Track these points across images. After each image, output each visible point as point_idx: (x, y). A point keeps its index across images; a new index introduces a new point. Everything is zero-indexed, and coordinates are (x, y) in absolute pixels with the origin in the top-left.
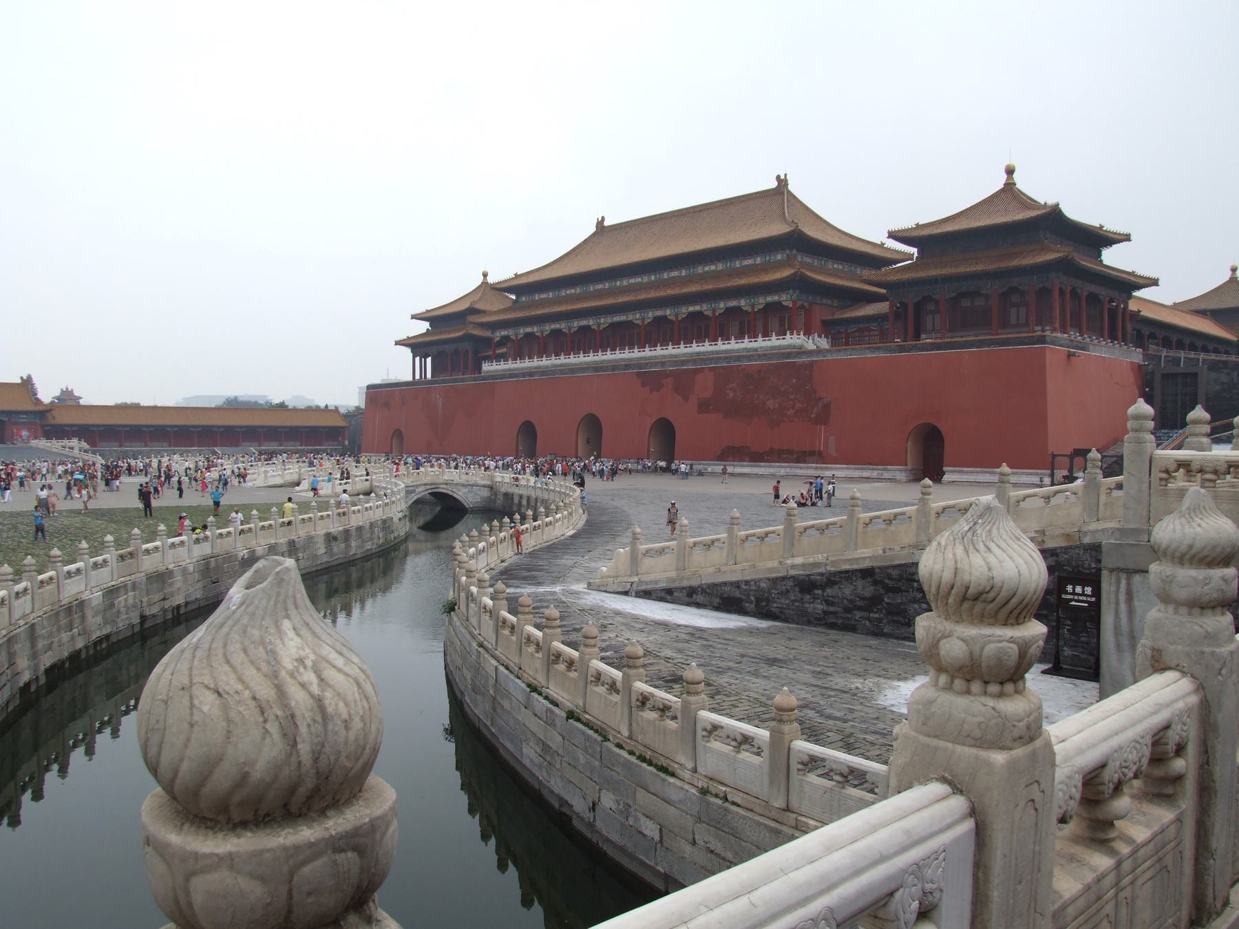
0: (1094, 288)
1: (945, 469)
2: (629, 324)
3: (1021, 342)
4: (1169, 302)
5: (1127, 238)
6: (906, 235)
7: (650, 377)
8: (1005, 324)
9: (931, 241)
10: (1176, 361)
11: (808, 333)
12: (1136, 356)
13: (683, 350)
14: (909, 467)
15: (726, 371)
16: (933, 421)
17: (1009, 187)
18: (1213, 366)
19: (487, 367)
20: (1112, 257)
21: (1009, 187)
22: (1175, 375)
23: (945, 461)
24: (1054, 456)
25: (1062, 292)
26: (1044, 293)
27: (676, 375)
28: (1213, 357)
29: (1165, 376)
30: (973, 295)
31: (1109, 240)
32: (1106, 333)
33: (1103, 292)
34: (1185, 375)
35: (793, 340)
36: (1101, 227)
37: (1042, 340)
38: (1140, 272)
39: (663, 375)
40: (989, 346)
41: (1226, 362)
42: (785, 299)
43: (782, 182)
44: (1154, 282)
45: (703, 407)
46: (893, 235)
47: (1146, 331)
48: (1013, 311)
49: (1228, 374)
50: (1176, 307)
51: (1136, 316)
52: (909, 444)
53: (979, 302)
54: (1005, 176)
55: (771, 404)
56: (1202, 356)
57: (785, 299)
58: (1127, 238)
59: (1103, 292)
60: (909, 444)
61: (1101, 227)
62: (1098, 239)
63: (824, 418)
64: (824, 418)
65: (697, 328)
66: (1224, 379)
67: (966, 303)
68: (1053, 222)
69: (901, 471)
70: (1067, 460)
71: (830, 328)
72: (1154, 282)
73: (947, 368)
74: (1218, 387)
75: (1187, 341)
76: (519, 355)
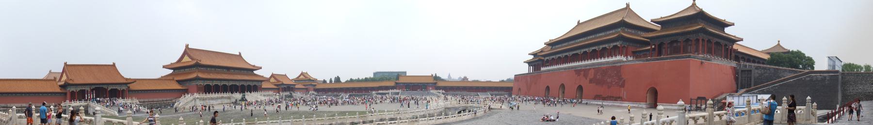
2: (577, 54)
3: (683, 57)
7: (578, 71)
8: (685, 51)
9: (665, 23)
11: (626, 55)
13: (583, 63)
15: (598, 69)
19: (543, 69)
25: (703, 40)
26: (698, 40)
27: (584, 70)
30: (676, 41)
35: (618, 58)
39: (581, 71)
42: (618, 44)
43: (628, 5)
45: (591, 81)
55: (609, 80)
57: (618, 44)
63: (623, 86)
64: (623, 86)
65: (595, 55)
67: (675, 45)
68: (701, 16)
71: (635, 54)
73: (663, 67)
76: (551, 65)
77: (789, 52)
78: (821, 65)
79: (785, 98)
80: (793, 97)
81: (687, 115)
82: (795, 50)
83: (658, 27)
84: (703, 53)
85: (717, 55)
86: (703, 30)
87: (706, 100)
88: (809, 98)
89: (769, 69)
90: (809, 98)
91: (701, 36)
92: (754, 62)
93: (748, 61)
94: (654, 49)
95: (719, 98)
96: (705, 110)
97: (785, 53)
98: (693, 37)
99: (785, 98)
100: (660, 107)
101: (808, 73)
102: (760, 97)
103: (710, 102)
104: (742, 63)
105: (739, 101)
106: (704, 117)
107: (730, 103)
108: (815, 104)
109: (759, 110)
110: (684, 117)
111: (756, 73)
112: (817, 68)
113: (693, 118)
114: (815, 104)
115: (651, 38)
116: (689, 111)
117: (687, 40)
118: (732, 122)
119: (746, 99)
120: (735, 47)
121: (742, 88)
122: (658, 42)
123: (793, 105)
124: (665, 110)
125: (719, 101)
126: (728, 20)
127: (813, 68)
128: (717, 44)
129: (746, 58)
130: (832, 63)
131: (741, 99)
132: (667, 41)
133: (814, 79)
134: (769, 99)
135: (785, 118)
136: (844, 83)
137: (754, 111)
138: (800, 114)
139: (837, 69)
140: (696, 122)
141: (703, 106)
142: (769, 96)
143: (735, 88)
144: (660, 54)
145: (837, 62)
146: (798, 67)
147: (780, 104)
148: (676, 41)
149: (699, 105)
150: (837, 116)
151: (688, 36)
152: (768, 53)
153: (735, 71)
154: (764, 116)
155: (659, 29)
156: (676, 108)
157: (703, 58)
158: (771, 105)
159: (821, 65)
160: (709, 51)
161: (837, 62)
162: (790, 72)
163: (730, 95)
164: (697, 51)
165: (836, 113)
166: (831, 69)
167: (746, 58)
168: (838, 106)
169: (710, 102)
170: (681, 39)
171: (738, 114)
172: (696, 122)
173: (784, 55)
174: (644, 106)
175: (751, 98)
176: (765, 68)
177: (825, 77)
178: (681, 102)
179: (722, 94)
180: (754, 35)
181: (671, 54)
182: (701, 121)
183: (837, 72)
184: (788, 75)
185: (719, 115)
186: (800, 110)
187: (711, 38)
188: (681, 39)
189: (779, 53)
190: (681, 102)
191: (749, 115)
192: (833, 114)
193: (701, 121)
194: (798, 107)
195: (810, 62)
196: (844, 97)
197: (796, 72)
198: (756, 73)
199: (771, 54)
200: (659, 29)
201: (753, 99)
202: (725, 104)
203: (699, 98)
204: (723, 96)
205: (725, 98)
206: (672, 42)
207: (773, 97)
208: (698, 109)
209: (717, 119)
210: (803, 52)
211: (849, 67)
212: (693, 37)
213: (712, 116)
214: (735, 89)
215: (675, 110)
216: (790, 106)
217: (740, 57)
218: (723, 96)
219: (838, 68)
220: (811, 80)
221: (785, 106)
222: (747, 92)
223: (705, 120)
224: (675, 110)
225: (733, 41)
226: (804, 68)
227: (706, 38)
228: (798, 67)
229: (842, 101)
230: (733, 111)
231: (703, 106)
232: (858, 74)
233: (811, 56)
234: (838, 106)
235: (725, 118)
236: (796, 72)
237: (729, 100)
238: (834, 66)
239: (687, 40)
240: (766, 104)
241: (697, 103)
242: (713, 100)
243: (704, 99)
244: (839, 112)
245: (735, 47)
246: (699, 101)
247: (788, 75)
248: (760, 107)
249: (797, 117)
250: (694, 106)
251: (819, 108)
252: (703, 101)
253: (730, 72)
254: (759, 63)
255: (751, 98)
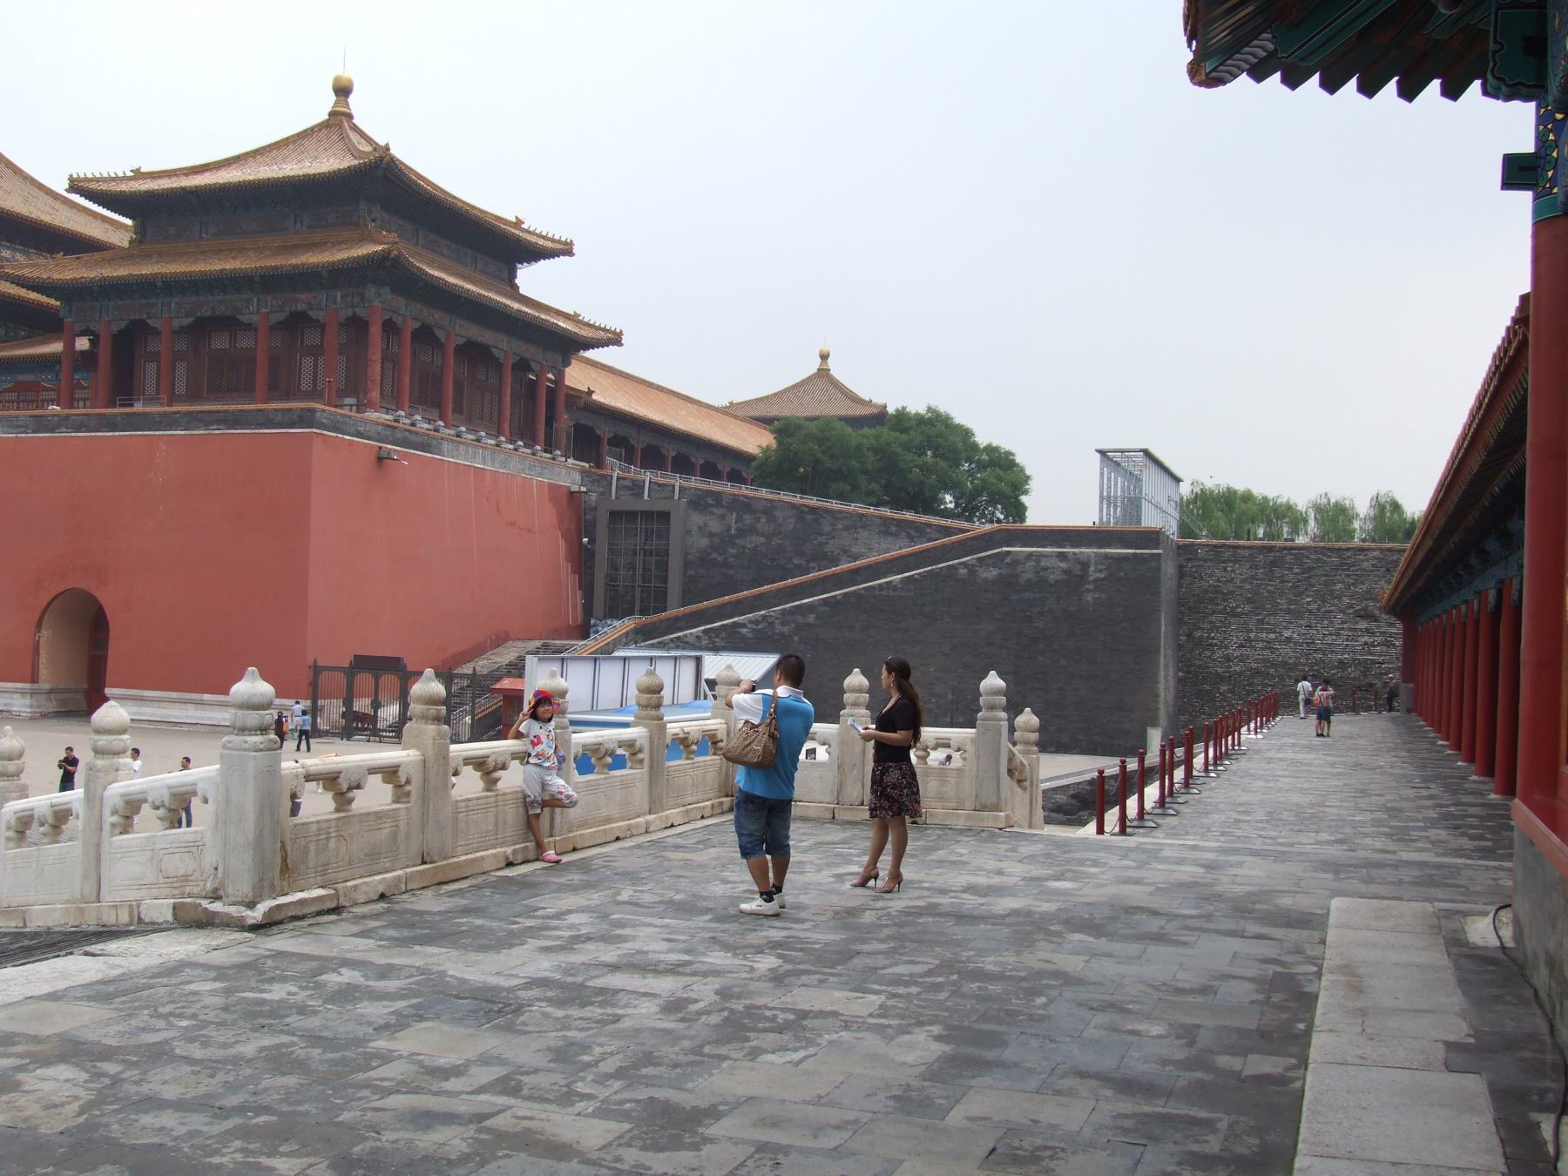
0: (484, 336)
1: (108, 691)
4: (720, 401)
5: (566, 250)
6: (93, 186)
8: (282, 386)
9: (162, 209)
10: (637, 487)
12: (568, 473)
14: (45, 685)
16: (83, 584)
17: (339, 121)
18: (699, 502)
20: (533, 280)
21: (339, 121)
22: (632, 515)
23: (110, 674)
24: (317, 670)
25: (390, 327)
26: (358, 326)
28: (696, 483)
29: (615, 516)
30: (230, 324)
31: (535, 252)
32: (506, 426)
33: (504, 346)
34: (648, 515)
36: (518, 223)
37: (306, 419)
38: (588, 316)
40: (207, 425)
41: (719, 493)
44: (615, 339)
46: (76, 186)
47: (605, 431)
48: (308, 363)
49: (722, 517)
50: (730, 411)
51: (581, 402)
52: (45, 634)
53: (245, 342)
54: (332, 98)
56: (678, 481)
58: (566, 250)
59: (504, 346)
60: (45, 634)
61: (518, 223)
62: (507, 248)
66: (715, 526)
67: (220, 342)
68: (383, 187)
69: (23, 693)
70: (341, 679)
72: (615, 339)
74: (704, 542)
75: (671, 451)
77: (879, 417)
78: (1063, 498)
79: (856, 679)
80: (901, 672)
81: (291, 762)
82: (917, 407)
83: (117, 229)
84: (393, 399)
85: (472, 422)
86: (387, 271)
87: (407, 677)
88: (993, 681)
89: (769, 509)
90: (993, 681)
91: (380, 303)
92: (683, 466)
93: (652, 459)
94: (87, 360)
95: (483, 665)
96: (396, 732)
97: (855, 422)
98: (329, 307)
99: (856, 679)
100: (112, 712)
101: (988, 540)
102: (715, 664)
103: (429, 686)
104: (615, 468)
105: (596, 688)
106: (390, 773)
107: (543, 698)
108: (1028, 718)
109: (711, 741)
110: (273, 771)
111: (692, 533)
112: (1041, 511)
113: (330, 780)
114: (1028, 718)
115: (70, 292)
116: (305, 735)
117: (297, 323)
118: (553, 802)
119: (638, 673)
120: (576, 377)
121: (615, 610)
122: (112, 320)
123: (900, 721)
124: (137, 725)
125: (481, 685)
126: (539, 221)
127: (1018, 511)
128: (474, 353)
129: (640, 441)
130: (1119, 486)
131: (610, 673)
132: (169, 316)
133: (1027, 575)
134: (766, 681)
135: (860, 788)
136: (1191, 608)
137: (683, 743)
138: (941, 773)
139: (1150, 519)
140: (343, 801)
141: (390, 712)
142: (756, 665)
143: (572, 613)
144: (124, 388)
145: (1152, 484)
146: (929, 504)
147: (830, 710)
148: (230, 324)
149: (362, 705)
150: (1152, 792)
151: (302, 301)
152: (765, 421)
153: (577, 515)
154: (740, 777)
155: (121, 239)
156: (224, 716)
157: (390, 433)
158: (777, 713)
159: (1063, 498)
160: (428, 396)
161: (1152, 484)
162: (889, 529)
163: (547, 652)
164: (354, 387)
165: (1145, 776)
166: (1114, 520)
167: (640, 441)
168: (1155, 738)
169: (429, 686)
170: (258, 310)
171: (588, 760)
172: (343, 801)
173: (854, 436)
174: (21, 704)
175: (664, 672)
176: (745, 506)
177: (1085, 565)
178: (253, 686)
179: (500, 640)
180: (690, 316)
181: (194, 396)
182: (375, 797)
183: (1153, 537)
184: (874, 545)
185: (480, 763)
186: (941, 749)
187: (437, 318)
188: (258, 310)
189: (826, 423)
190: (253, 686)
191: (655, 771)
192: (1130, 783)
193: (375, 797)
194: (928, 733)
195: (1001, 479)
196: (1193, 682)
197: (920, 531)
198: (692, 533)
199: (784, 428)
200: (121, 239)
201: (675, 676)
202: (515, 698)
203: (363, 663)
204: (506, 655)
205: (517, 669)
206: (202, 328)
207: (791, 671)
208: (358, 726)
209: (468, 784)
210: (959, 418)
211: (1222, 510)
212: (329, 307)
213: (439, 770)
214: (573, 615)
215: (216, 729)
216: (884, 722)
217: (602, 434)
218: (506, 655)
219: (1160, 516)
220: (1007, 583)
221: (858, 720)
222: (641, 635)
223: (401, 793)
224: (216, 729)
225: (565, 341)
226: (968, 509)
227: (410, 314)
228: (929, 504)
229: (1181, 706)
230: (560, 745)
231: (390, 712)
232: (1277, 557)
233: (1004, 442)
234: (1155, 738)
235: (513, 778)
236: (920, 531)
237: (540, 677)
238: (1133, 505)
239: (297, 323)
240: (749, 706)
241: (353, 690)
242: (445, 676)
243: (391, 671)
244: (1165, 769)
245: (576, 377)
246: (364, 679)
247: (874, 545)
248: (716, 724)
249: (928, 788)
250: (333, 709)
251: (1051, 742)
252: (389, 680)
253: (546, 517)
254: (710, 471)
255: (664, 672)
